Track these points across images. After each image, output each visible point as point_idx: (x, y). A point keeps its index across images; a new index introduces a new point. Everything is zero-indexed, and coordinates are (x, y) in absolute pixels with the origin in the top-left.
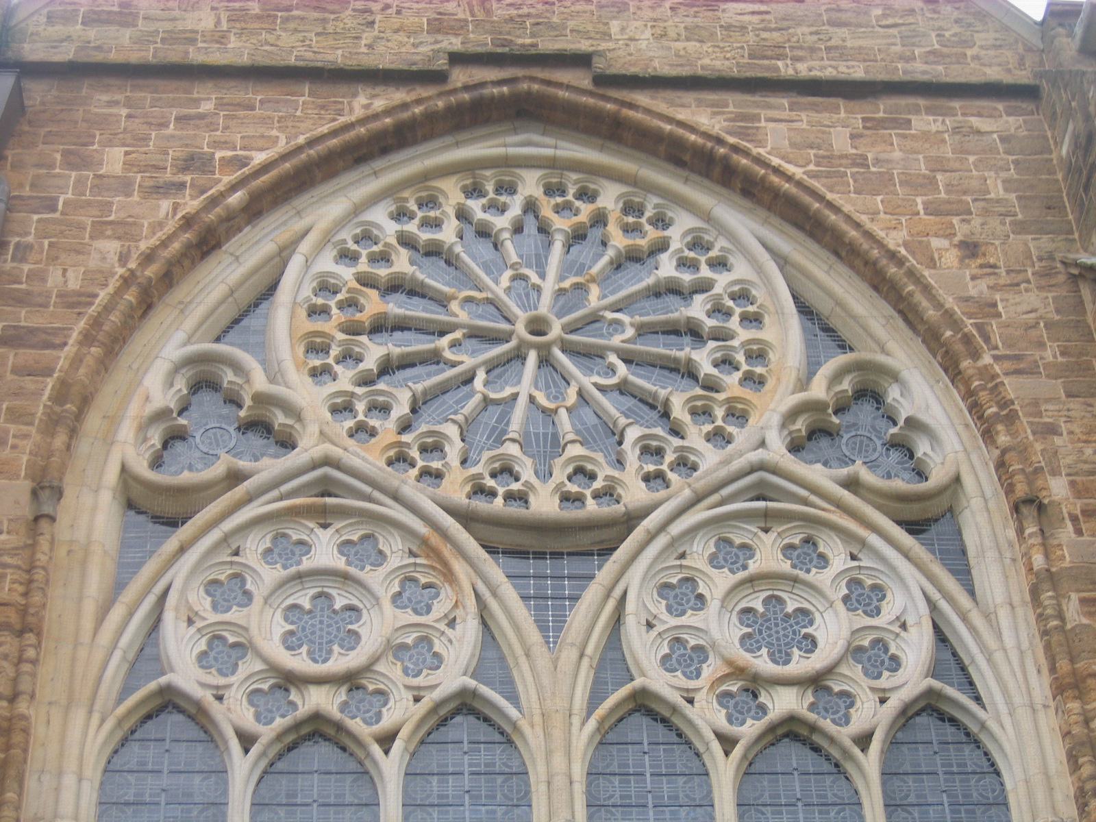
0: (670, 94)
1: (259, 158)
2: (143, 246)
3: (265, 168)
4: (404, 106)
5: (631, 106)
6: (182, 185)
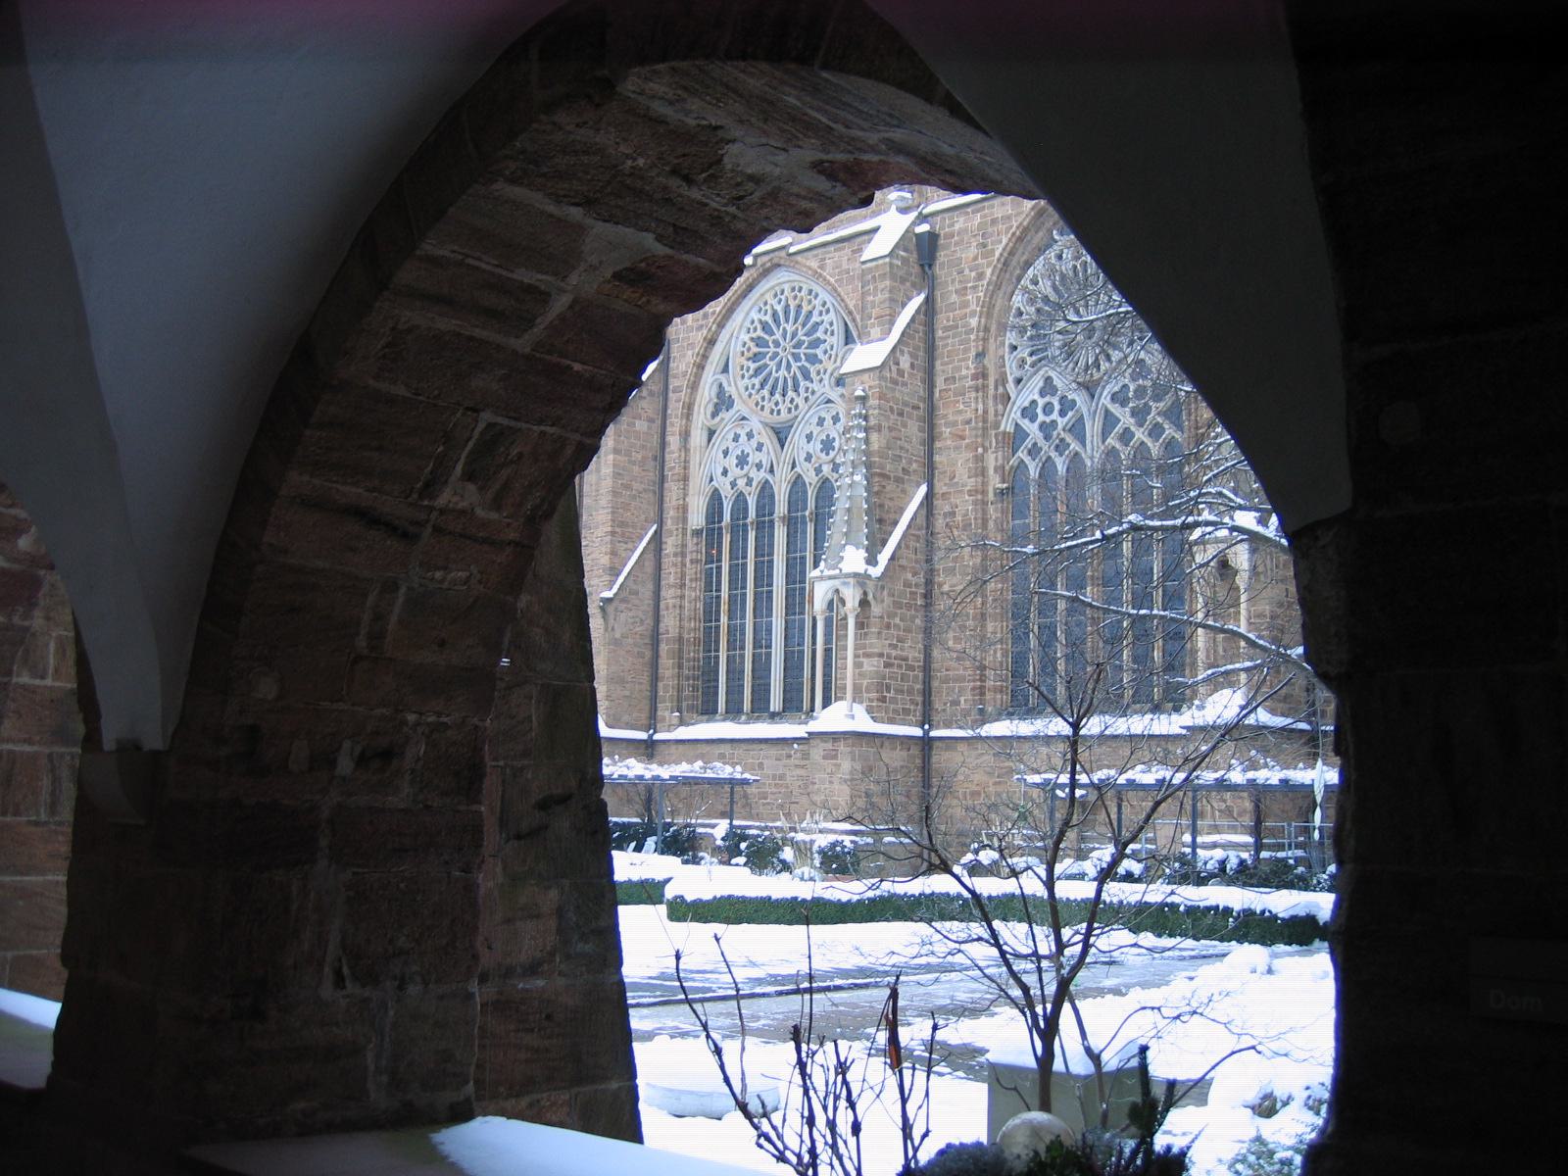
0: (805, 254)
1: (718, 309)
2: (697, 350)
3: (721, 311)
4: (748, 278)
5: (797, 262)
6: (702, 326)
